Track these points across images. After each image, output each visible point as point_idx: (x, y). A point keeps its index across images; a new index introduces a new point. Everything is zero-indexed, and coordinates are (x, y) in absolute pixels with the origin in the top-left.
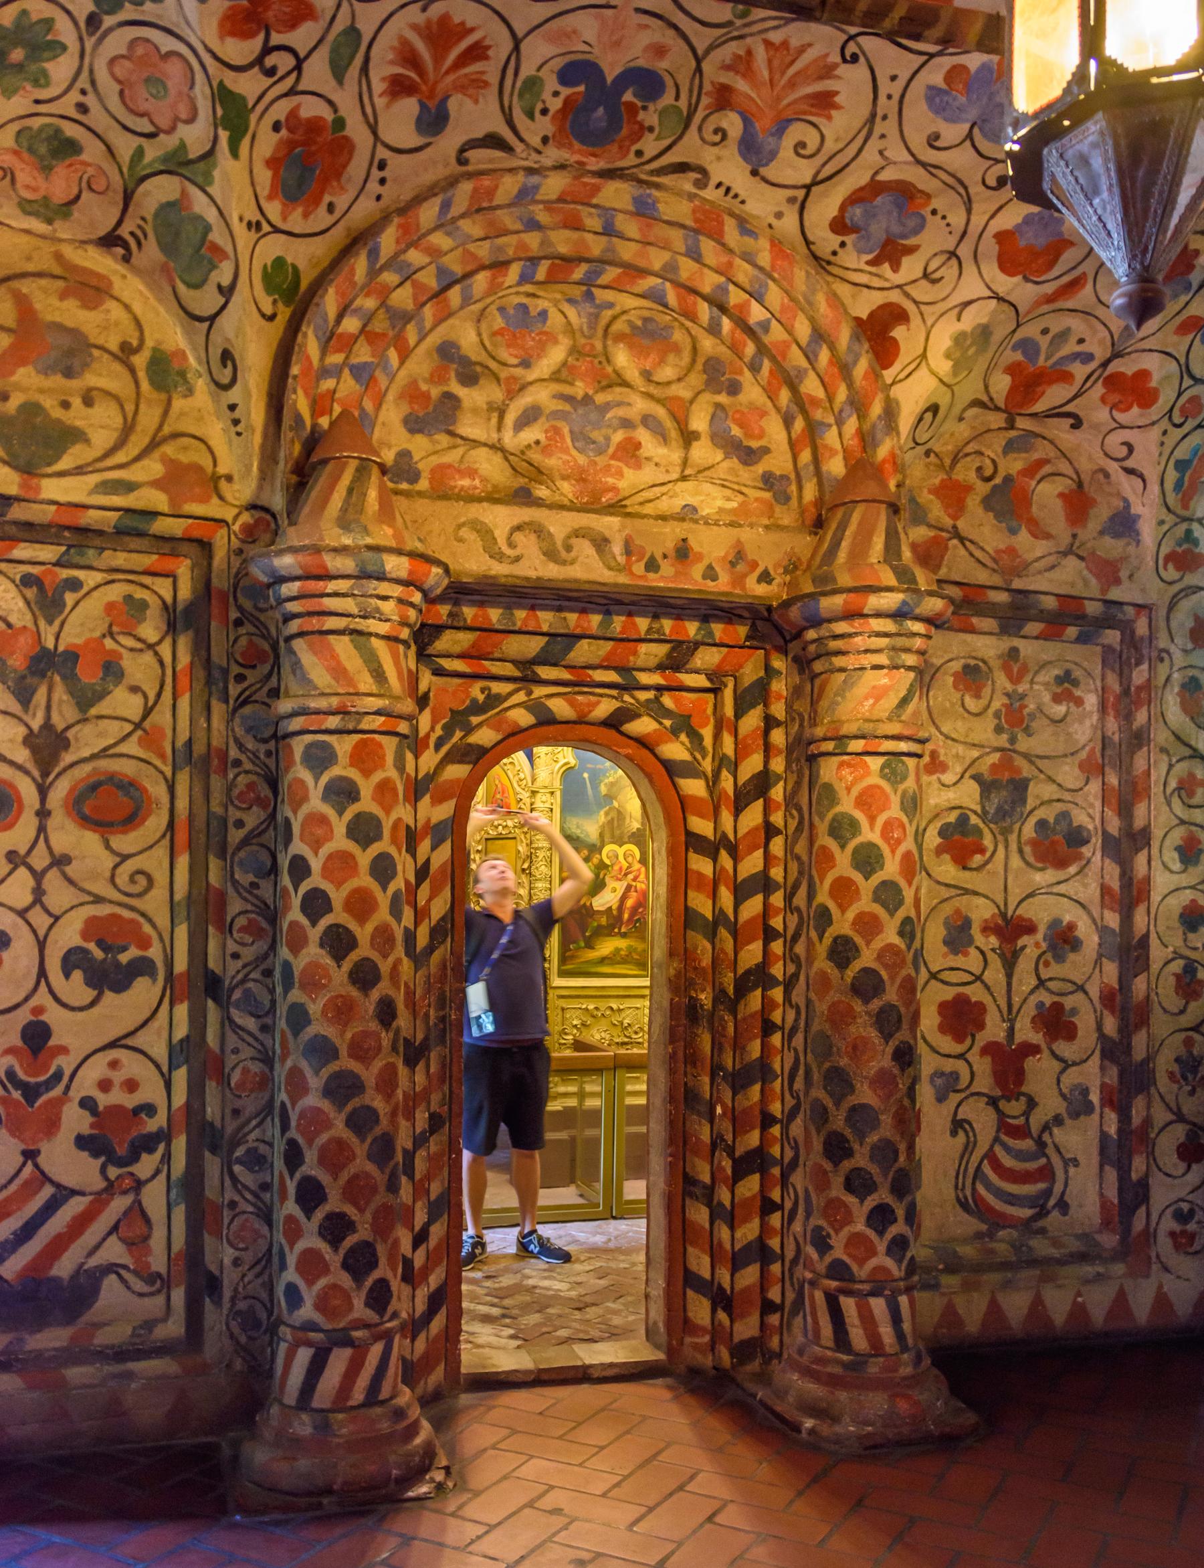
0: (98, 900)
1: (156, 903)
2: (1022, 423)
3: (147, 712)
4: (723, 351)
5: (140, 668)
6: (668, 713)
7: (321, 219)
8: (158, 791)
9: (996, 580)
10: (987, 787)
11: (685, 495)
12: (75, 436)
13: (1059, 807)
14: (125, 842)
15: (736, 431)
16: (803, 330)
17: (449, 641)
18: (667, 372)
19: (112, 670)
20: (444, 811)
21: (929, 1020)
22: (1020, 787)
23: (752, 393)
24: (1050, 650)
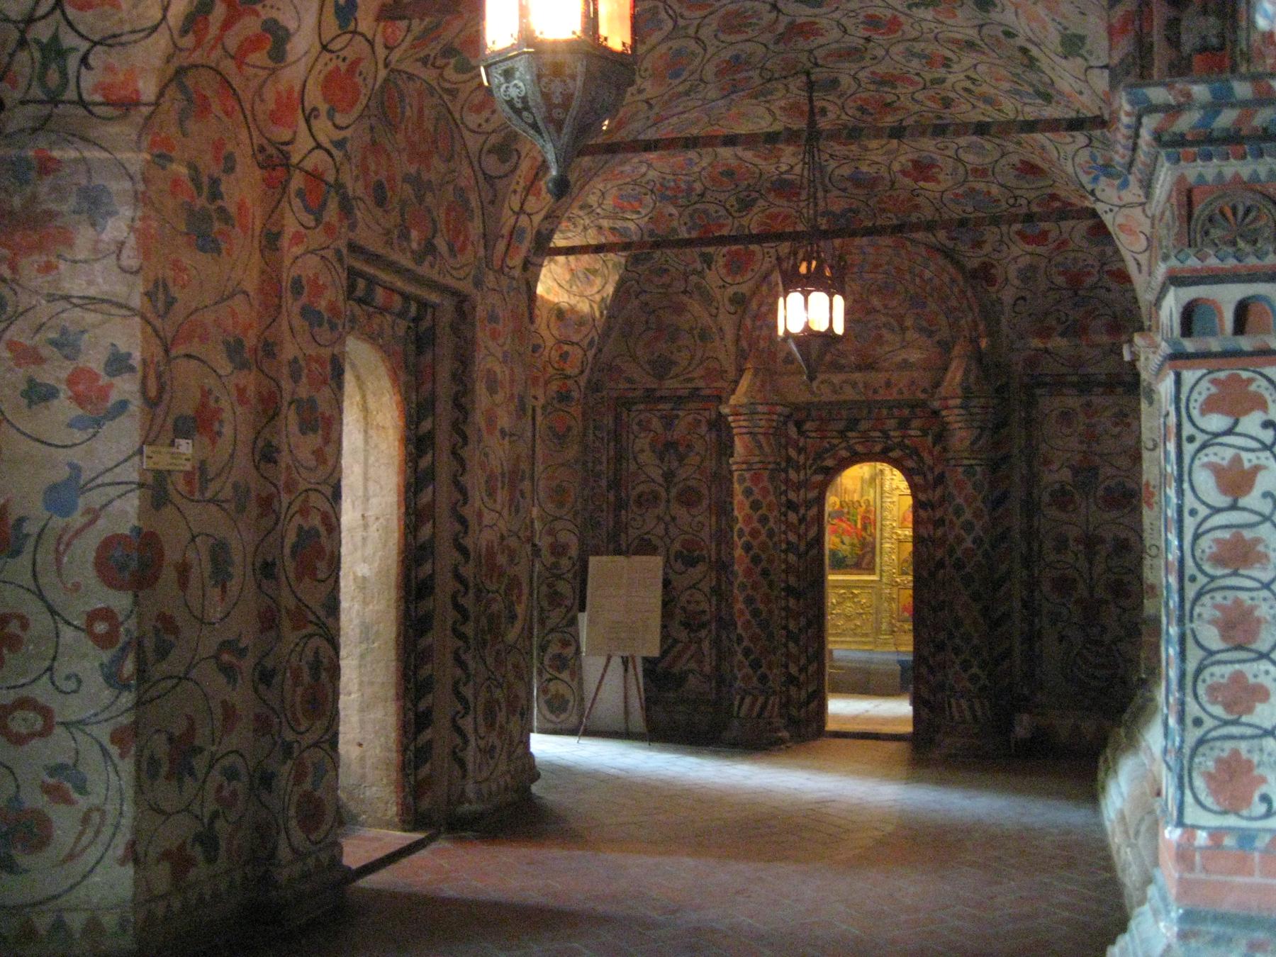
0: (686, 533)
1: (705, 534)
2: (1080, 292)
3: (702, 461)
4: (919, 290)
5: (699, 446)
6: (907, 447)
7: (750, 275)
8: (705, 492)
9: (1071, 370)
10: (1076, 471)
11: (903, 355)
12: (675, 363)
13: (1117, 480)
14: (694, 511)
15: (925, 324)
16: (946, 278)
17: (808, 426)
18: (895, 303)
19: (689, 447)
20: (812, 494)
21: (1046, 587)
22: (1094, 470)
23: (932, 306)
24: (1110, 400)
